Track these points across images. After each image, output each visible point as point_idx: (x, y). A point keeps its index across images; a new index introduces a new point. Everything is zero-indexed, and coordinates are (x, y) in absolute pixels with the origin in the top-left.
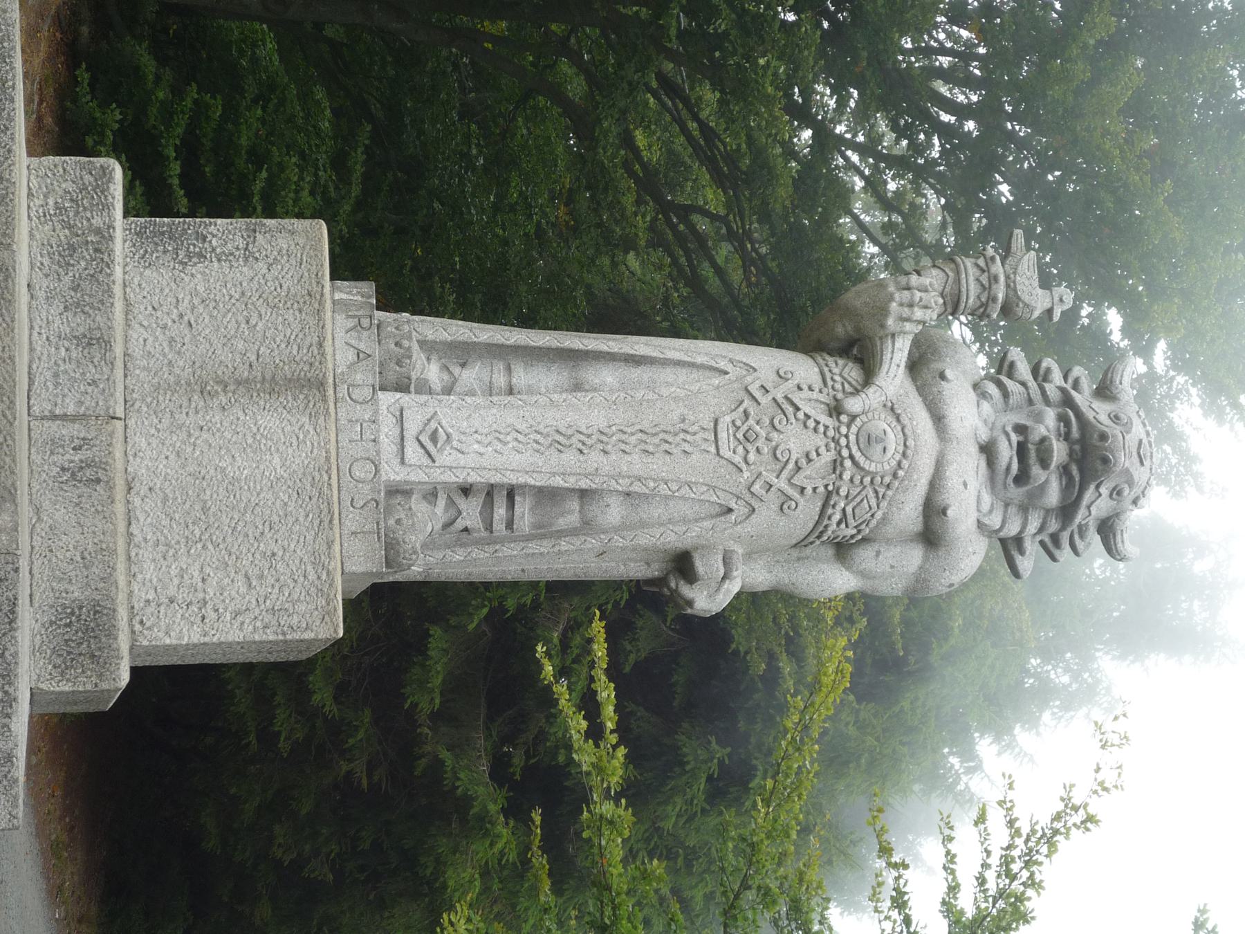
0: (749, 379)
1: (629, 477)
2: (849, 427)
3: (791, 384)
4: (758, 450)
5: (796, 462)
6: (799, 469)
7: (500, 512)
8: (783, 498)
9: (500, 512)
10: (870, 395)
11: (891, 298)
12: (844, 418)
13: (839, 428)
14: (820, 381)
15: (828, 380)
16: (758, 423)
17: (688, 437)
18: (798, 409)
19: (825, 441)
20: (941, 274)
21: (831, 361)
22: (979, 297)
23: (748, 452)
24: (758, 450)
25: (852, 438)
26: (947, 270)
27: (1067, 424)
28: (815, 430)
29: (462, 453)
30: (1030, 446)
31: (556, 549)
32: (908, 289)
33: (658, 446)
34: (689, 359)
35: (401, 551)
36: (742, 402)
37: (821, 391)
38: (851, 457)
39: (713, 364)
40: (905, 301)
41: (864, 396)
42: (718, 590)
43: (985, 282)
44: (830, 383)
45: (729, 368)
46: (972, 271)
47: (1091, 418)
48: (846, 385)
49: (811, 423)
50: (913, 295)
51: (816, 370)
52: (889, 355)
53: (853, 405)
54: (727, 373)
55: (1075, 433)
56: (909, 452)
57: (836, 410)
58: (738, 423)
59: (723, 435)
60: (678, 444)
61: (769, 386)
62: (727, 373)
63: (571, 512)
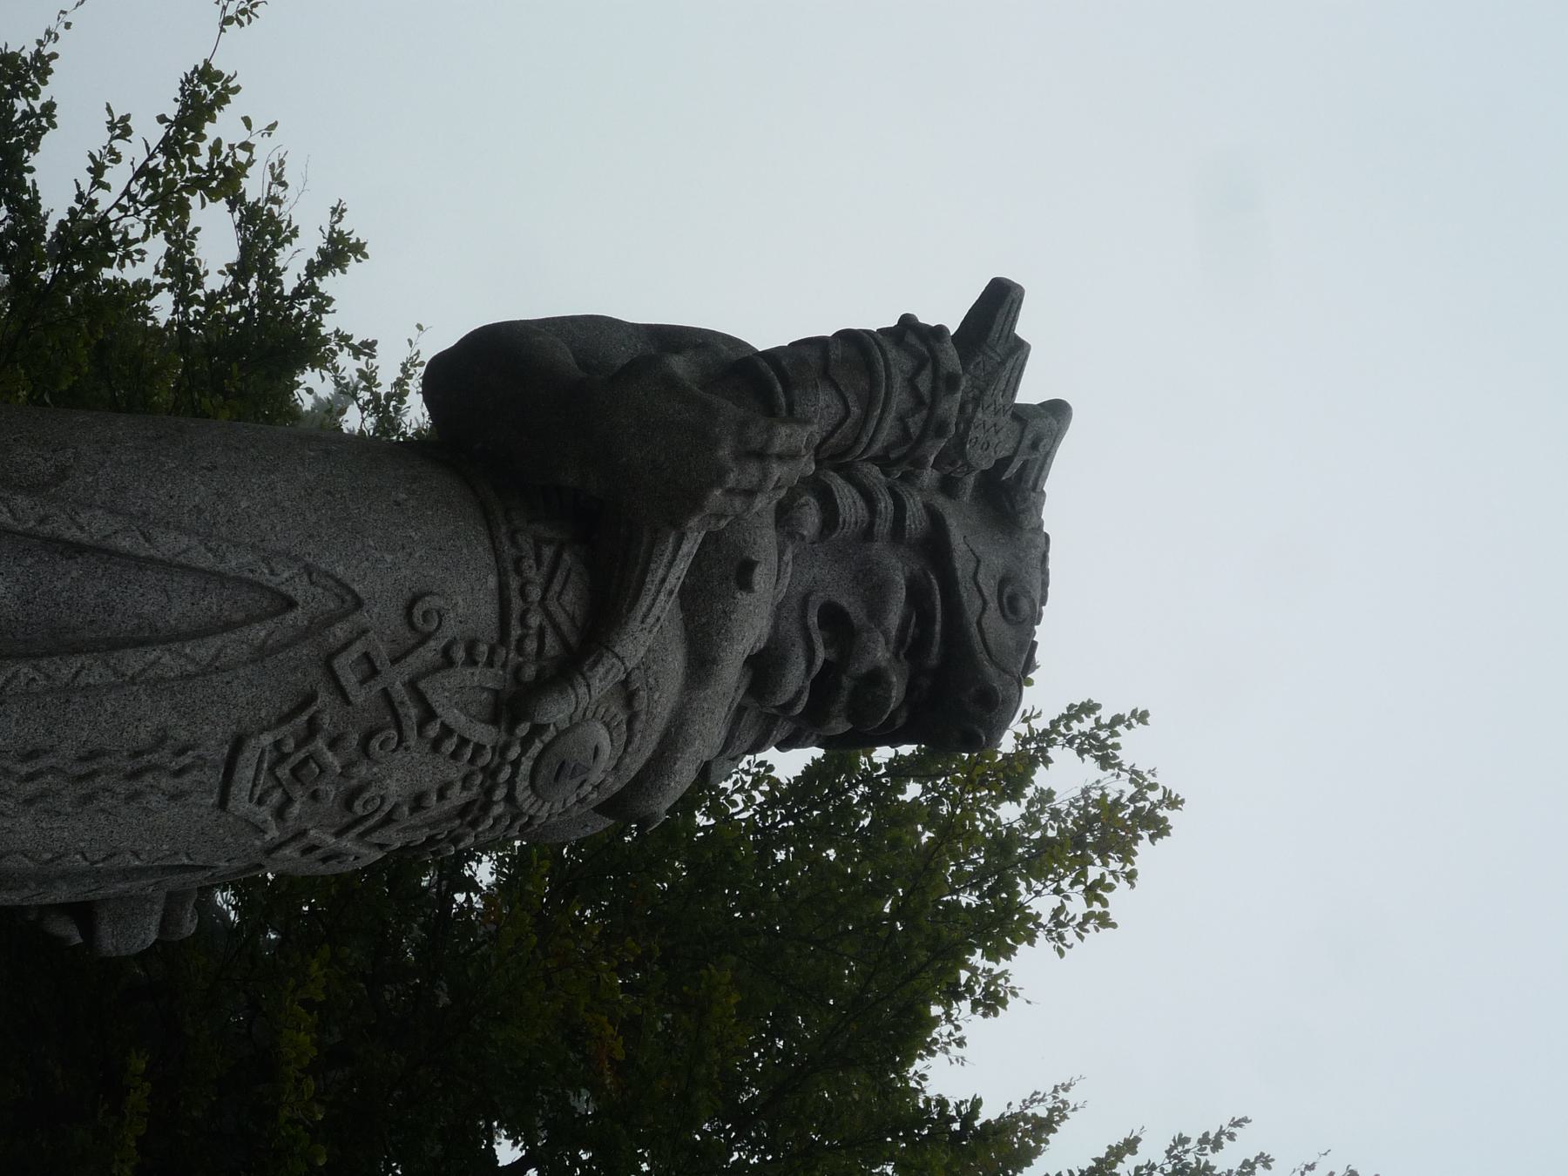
0: (340, 631)
2: (526, 743)
3: (429, 653)
4: (315, 796)
5: (391, 812)
6: (388, 820)
10: (596, 683)
11: (720, 476)
12: (523, 729)
13: (507, 747)
14: (494, 619)
15: (514, 622)
16: (333, 744)
17: (166, 782)
18: (429, 714)
19: (465, 770)
20: (836, 408)
21: (527, 545)
22: (887, 449)
23: (288, 801)
24: (315, 796)
25: (526, 766)
26: (851, 398)
27: (925, 619)
28: (455, 755)
30: (846, 682)
32: (761, 455)
33: (88, 799)
34: (205, 561)
36: (310, 698)
37: (490, 664)
38: (510, 798)
39: (263, 574)
40: (745, 485)
41: (582, 690)
43: (915, 427)
44: (516, 632)
45: (299, 589)
46: (900, 399)
47: (974, 629)
48: (550, 640)
49: (450, 745)
50: (765, 476)
51: (492, 581)
52: (661, 573)
53: (556, 711)
54: (291, 604)
55: (933, 660)
56: (628, 760)
57: (511, 708)
58: (290, 745)
59: (245, 772)
60: (134, 796)
61: (382, 652)
62: (291, 604)
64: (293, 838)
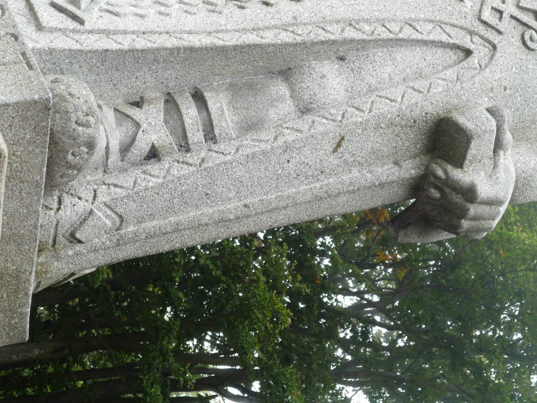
1: (338, 22)
7: (190, 113)
8: (520, 28)
9: (190, 113)
29: (116, 14)
31: (281, 141)
35: (71, 108)
42: (495, 166)
63: (281, 99)
64: (482, 5)
